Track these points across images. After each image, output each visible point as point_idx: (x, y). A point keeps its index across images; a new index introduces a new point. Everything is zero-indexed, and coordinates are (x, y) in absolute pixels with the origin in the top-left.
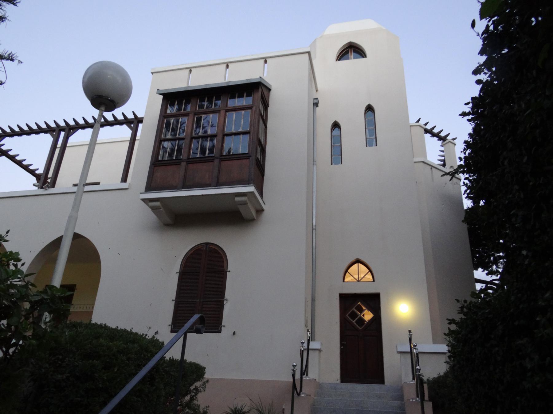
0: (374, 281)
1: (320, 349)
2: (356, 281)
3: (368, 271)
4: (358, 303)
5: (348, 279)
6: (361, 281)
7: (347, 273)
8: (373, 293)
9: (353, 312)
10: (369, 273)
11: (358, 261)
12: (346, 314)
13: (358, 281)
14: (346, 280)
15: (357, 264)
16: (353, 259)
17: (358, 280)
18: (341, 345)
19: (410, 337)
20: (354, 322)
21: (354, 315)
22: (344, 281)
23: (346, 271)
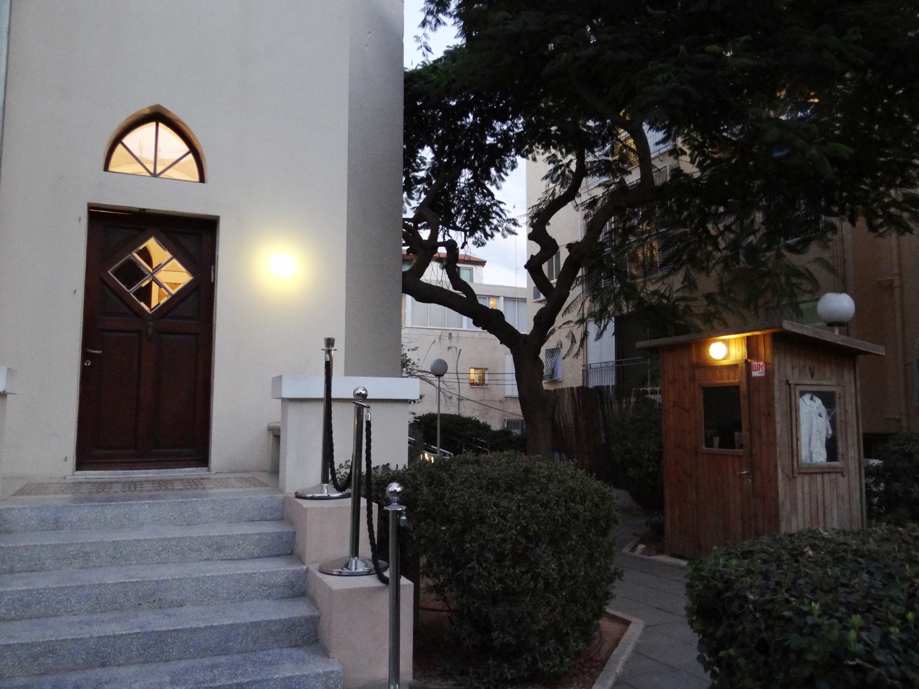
0: (202, 179)
1: (4, 391)
2: (148, 174)
3: (186, 149)
4: (146, 240)
5: (121, 162)
6: (161, 176)
7: (120, 146)
8: (198, 215)
9: (132, 264)
10: (191, 156)
11: (158, 116)
12: (109, 270)
13: (154, 175)
14: (111, 169)
15: (152, 125)
16: (143, 106)
17: (152, 170)
18: (85, 356)
19: (328, 359)
20: (131, 291)
21: (132, 273)
22: (106, 168)
23: (118, 140)
